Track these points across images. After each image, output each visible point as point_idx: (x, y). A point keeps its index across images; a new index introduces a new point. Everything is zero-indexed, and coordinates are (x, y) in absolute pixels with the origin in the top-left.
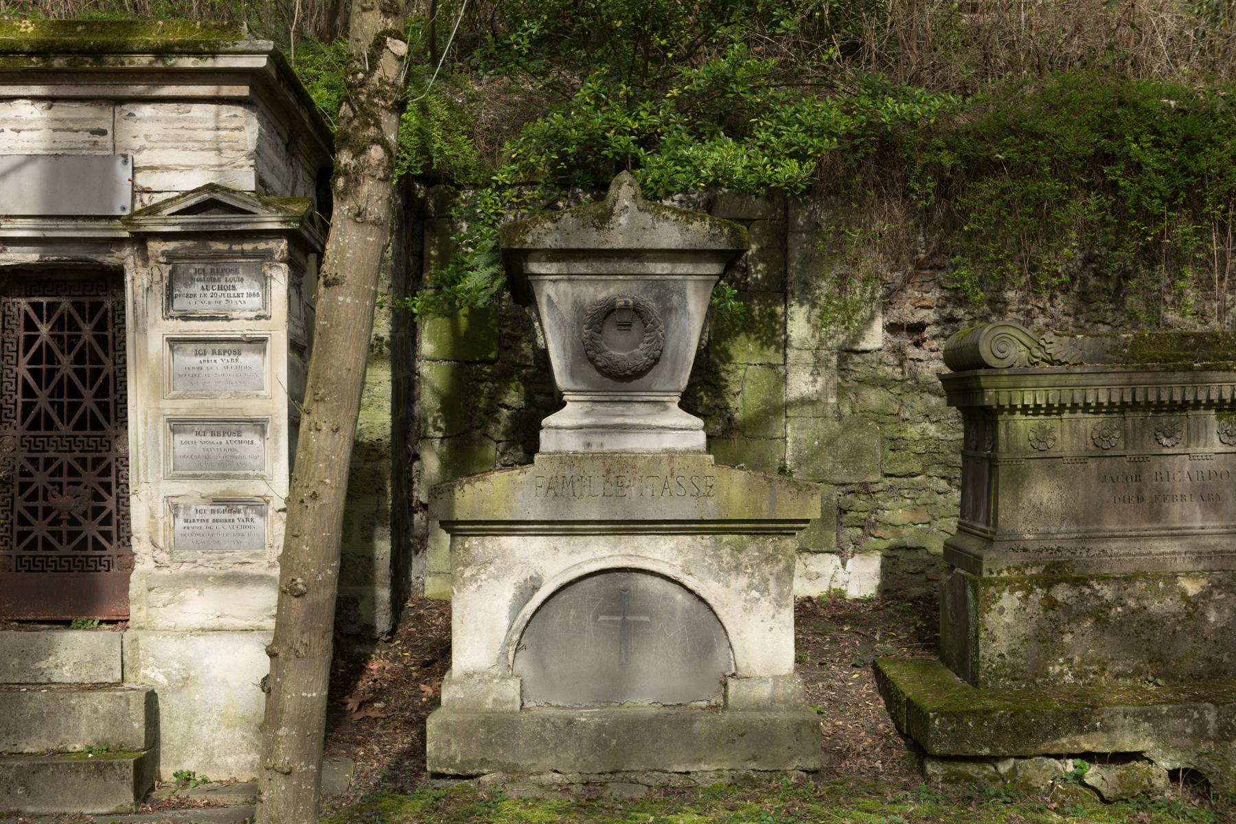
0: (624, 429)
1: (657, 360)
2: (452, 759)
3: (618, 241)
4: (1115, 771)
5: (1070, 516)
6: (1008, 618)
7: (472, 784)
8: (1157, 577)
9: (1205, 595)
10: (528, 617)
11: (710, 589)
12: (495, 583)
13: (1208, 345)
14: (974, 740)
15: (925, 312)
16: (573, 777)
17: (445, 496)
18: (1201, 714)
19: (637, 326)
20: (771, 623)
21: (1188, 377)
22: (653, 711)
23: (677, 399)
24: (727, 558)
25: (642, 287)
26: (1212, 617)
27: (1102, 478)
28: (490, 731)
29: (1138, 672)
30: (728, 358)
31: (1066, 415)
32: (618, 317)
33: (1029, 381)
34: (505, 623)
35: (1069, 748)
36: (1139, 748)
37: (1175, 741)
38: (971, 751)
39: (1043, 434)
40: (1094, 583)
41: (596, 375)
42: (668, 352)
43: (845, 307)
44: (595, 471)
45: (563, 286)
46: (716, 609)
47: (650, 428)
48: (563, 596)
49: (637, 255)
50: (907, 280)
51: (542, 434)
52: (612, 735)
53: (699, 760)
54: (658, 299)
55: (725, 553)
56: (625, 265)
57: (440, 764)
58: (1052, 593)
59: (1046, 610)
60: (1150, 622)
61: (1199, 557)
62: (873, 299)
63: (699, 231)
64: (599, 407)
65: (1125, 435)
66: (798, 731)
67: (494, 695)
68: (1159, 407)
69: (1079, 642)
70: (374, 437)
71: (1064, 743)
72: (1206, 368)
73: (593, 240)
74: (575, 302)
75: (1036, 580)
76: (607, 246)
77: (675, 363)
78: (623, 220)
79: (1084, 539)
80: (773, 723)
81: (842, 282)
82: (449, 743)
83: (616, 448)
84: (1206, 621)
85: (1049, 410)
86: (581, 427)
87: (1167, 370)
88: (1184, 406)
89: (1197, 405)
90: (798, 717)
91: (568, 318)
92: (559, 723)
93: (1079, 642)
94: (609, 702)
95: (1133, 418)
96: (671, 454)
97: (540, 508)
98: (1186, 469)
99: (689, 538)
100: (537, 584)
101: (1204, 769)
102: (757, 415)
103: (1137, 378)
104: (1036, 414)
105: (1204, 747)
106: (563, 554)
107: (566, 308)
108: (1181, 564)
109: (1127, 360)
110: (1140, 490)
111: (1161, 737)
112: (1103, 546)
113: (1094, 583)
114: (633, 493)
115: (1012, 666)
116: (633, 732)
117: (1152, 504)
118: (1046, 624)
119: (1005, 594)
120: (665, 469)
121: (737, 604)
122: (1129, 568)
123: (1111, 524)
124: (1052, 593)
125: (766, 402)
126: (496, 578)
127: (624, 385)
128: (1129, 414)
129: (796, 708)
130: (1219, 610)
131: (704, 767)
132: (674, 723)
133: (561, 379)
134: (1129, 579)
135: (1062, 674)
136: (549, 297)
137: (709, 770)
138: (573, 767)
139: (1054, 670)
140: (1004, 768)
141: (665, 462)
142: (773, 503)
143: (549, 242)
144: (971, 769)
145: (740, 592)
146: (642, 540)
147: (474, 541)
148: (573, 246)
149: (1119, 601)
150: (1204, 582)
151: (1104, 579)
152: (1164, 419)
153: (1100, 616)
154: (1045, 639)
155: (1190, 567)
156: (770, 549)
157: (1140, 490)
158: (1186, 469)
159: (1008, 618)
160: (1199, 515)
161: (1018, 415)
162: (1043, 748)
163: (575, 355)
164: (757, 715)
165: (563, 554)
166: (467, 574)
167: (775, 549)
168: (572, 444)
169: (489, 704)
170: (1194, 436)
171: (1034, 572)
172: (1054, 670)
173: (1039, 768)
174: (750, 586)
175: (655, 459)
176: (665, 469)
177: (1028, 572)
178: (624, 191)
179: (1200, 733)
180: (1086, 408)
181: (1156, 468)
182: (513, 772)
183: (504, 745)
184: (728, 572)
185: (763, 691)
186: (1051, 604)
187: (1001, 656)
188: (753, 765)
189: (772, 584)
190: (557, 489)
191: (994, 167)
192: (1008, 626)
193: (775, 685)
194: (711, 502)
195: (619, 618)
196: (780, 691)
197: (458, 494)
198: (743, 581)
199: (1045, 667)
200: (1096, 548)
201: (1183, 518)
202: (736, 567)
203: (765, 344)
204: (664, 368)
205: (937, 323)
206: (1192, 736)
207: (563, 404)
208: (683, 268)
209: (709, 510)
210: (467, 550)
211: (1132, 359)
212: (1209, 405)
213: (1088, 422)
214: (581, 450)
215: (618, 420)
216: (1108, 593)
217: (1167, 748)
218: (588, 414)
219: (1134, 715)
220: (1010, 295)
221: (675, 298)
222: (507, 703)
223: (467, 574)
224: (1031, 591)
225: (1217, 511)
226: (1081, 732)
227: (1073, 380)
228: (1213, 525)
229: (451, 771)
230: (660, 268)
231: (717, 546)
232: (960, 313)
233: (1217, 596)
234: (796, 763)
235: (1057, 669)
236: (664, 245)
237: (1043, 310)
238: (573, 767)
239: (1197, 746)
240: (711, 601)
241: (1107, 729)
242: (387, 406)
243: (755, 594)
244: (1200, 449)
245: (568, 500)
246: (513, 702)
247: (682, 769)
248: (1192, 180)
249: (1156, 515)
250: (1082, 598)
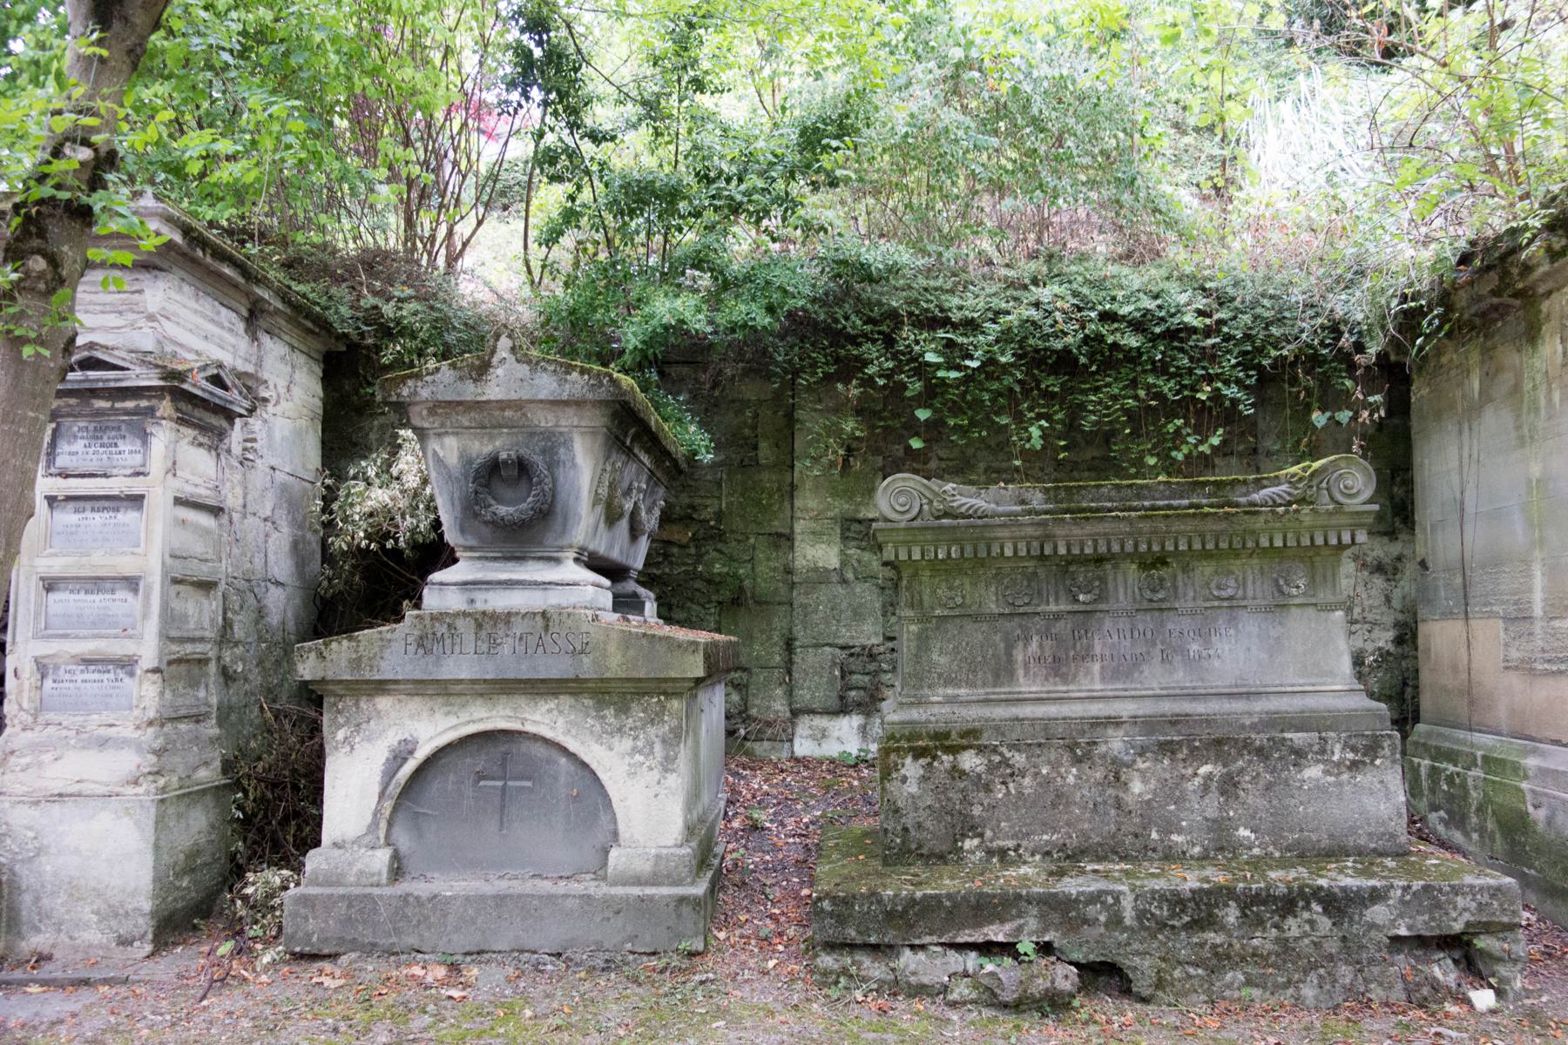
2: (309, 935)
6: (912, 788)
12: (366, 745)
20: (657, 789)
26: (1137, 787)
28: (350, 906)
34: (376, 789)
41: (486, 531)
46: (599, 774)
51: (426, 591)
63: (576, 384)
67: (359, 866)
73: (469, 391)
76: (484, 398)
78: (500, 371)
82: (306, 919)
86: (466, 583)
91: (456, 473)
100: (410, 747)
121: (621, 768)
126: (369, 740)
130: (1145, 781)
136: (435, 452)
159: (912, 788)
164: (636, 891)
174: (635, 750)
183: (365, 922)
184: (611, 734)
194: (586, 660)
195: (499, 784)
198: (627, 744)
202: (620, 730)
207: (456, 561)
222: (373, 875)
240: (594, 766)
243: (639, 758)
245: (438, 658)
246: (379, 874)
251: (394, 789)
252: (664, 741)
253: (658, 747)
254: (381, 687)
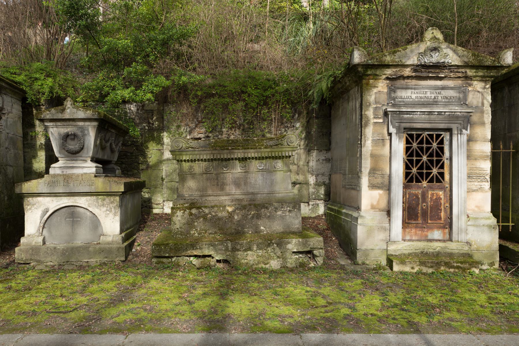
0: (73, 167)
1: (82, 149)
2: (22, 259)
3: (67, 116)
4: (200, 260)
5: (198, 190)
6: (179, 218)
7: (27, 266)
8: (220, 206)
9: (234, 211)
10: (45, 219)
11: (96, 211)
12: (36, 210)
13: (235, 143)
14: (164, 252)
15: (201, 135)
16: (56, 263)
17: (20, 186)
18: (227, 244)
19: (76, 139)
21: (228, 151)
22: (80, 245)
23: (90, 159)
24: (100, 202)
25: (77, 128)
26: (236, 217)
27: (207, 179)
28: (33, 251)
29: (216, 233)
30: (148, 148)
31: (197, 162)
32: (70, 137)
33: (184, 153)
34: (39, 221)
35: (190, 254)
36: (210, 254)
37: (220, 252)
38: (163, 255)
39: (191, 167)
40: (203, 208)
41: (66, 153)
42: (86, 146)
43: (179, 134)
44: (61, 179)
45: (55, 129)
47: (80, 167)
48: (56, 213)
49: (73, 120)
50: (196, 126)
51: (50, 169)
52: (67, 252)
53: (91, 258)
54: (81, 132)
55: (100, 201)
56: (71, 123)
57: (19, 260)
58: (191, 211)
59: (190, 216)
60: (219, 219)
61: (232, 201)
62: (186, 131)
63: (89, 114)
64: (68, 162)
65: (213, 167)
66: (118, 250)
68: (222, 160)
69: (199, 224)
70: (40, 171)
71: (189, 252)
72: (233, 149)
73: (60, 116)
74: (59, 133)
75: (187, 208)
76: (64, 118)
77: (88, 149)
78: (68, 111)
79: (202, 196)
80: (111, 248)
81: (179, 127)
82: (21, 254)
83: (70, 173)
84: (234, 219)
85: (192, 161)
87: (222, 150)
88: (229, 159)
89: (232, 159)
90: (118, 246)
91: (57, 137)
92: (52, 248)
93: (199, 224)
94: (69, 243)
95: (215, 163)
96: (86, 174)
97: (46, 190)
98: (231, 176)
99: (89, 197)
101: (229, 260)
102: (155, 163)
103: (214, 152)
104: (188, 162)
105: (228, 253)
106: (55, 202)
107: (56, 135)
108: (227, 203)
109: (212, 147)
110: (218, 183)
111: (216, 250)
112: (207, 198)
113: (203, 208)
114: (72, 185)
115: (181, 231)
116: (73, 251)
117: (221, 186)
118: (190, 220)
119: (178, 212)
120: (80, 178)
121: (103, 215)
122: (213, 204)
123: (210, 192)
124: (191, 211)
125: (158, 160)
126: (36, 209)
127: (74, 155)
128: (214, 162)
129: (119, 243)
130: (238, 215)
131: (92, 260)
132: (85, 248)
133: (57, 154)
134: (213, 207)
135: (194, 233)
136: (51, 132)
137: (94, 261)
138: (56, 260)
139: (192, 232)
140: (173, 259)
141: (80, 176)
142: (110, 187)
143: (48, 117)
144: (165, 260)
145: (104, 212)
146: (77, 198)
147: (30, 199)
148: (55, 118)
149: (210, 213)
150: (233, 208)
151: (206, 207)
152: (224, 163)
153: (205, 217)
154: (190, 224)
155: (230, 204)
156: (112, 200)
157: (218, 183)
158: (231, 176)
159: (179, 218)
160: (234, 189)
161: (183, 162)
162: (183, 254)
163: (60, 147)
165: (55, 202)
166: (28, 208)
167: (114, 200)
168: (58, 172)
169: (34, 243)
170: (233, 168)
171: (187, 205)
172: (192, 232)
173: (183, 259)
174: (107, 210)
175: (78, 176)
176: (80, 178)
177: (185, 205)
178: (68, 103)
179: (227, 250)
180: (202, 160)
181: (222, 177)
182: (39, 262)
184: (101, 206)
185: (110, 239)
186: (191, 214)
187: (177, 228)
188: (106, 259)
189: (113, 209)
190: (52, 184)
191: (213, 95)
192: (179, 220)
193: (113, 237)
194: (93, 187)
196: (115, 239)
197: (23, 186)
198: (105, 209)
199: (190, 232)
200: (204, 199)
201: (230, 190)
203: (158, 144)
204: (85, 150)
205: (204, 138)
206: (225, 250)
207: (59, 161)
208: (87, 123)
209: (93, 189)
210: (28, 201)
211: (214, 147)
212: (236, 159)
213: (204, 164)
214: (61, 173)
215: (71, 165)
216: (207, 211)
217: (217, 254)
218: (64, 163)
219: (208, 245)
220: (224, 130)
221: (86, 132)
223: (28, 208)
224: (185, 211)
225: (239, 188)
226: (193, 249)
227: (196, 152)
228: (238, 192)
229: (22, 262)
230: (81, 124)
231: (97, 199)
232: (210, 135)
233: (237, 212)
234: (118, 259)
235: (193, 232)
236: (80, 117)
237: (233, 134)
238: (56, 260)
239: (226, 253)
240: (96, 214)
241: (201, 249)
242: (44, 162)
243: (108, 212)
244: (234, 171)
247: (86, 261)
248: (265, 98)
249: (222, 189)
250: (199, 212)
251: (43, 221)
252: (114, 208)
253: (113, 209)
254: (39, 195)
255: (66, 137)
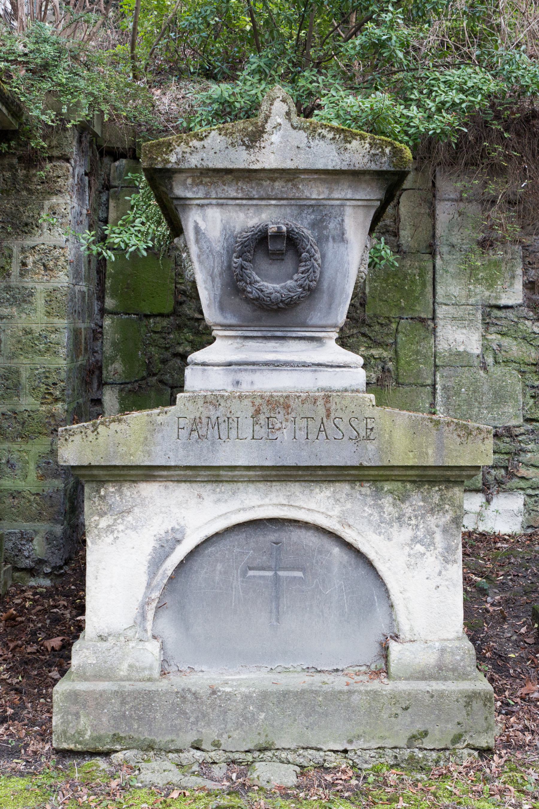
2: (81, 733)
20: (438, 580)
23: (335, 335)
28: (123, 703)
34: (144, 579)
41: (246, 309)
46: (377, 564)
49: (289, 175)
51: (188, 372)
54: (313, 225)
57: (67, 739)
66: (468, 704)
67: (129, 661)
73: (241, 159)
77: (332, 296)
78: (275, 138)
82: (77, 715)
86: (230, 364)
91: (218, 247)
100: (178, 536)
126: (134, 528)
133: (211, 314)
141: (320, 402)
143: (194, 161)
163: (225, 286)
164: (423, 686)
174: (415, 540)
183: (140, 718)
194: (371, 447)
195: (270, 574)
198: (407, 534)
202: (399, 518)
204: (323, 301)
209: (370, 455)
222: (144, 669)
229: (79, 747)
230: (315, 192)
236: (320, 166)
243: (419, 548)
245: (213, 443)
246: (151, 668)
251: (161, 578)
252: (445, 531)
253: (438, 537)
254: (149, 473)
255: (263, 244)
